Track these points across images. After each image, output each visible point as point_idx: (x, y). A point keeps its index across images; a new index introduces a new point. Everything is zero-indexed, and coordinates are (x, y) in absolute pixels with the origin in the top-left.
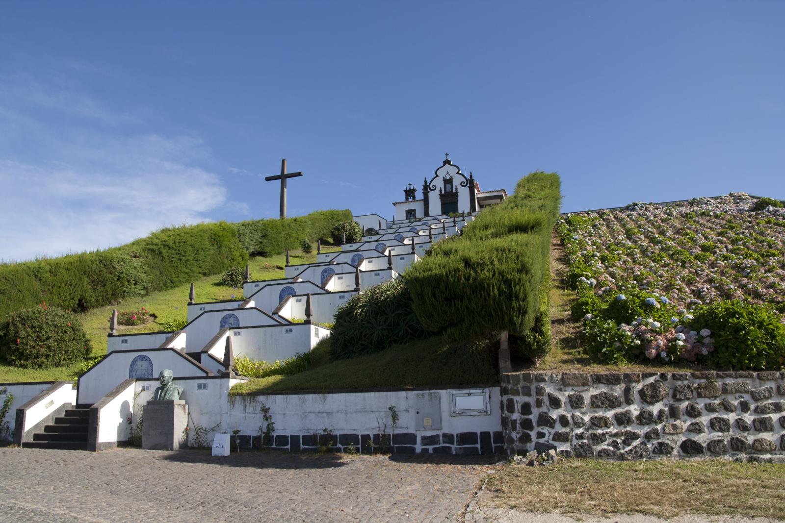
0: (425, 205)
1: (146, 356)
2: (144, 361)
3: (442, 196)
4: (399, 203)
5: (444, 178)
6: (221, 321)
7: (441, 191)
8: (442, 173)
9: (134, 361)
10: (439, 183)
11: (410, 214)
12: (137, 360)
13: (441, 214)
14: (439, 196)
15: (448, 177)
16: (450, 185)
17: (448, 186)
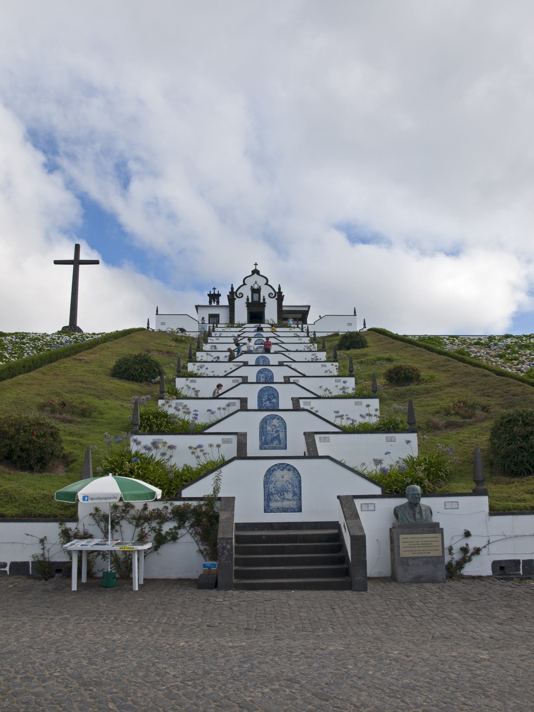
0: (230, 311)
1: (288, 465)
2: (285, 471)
3: (248, 305)
4: (202, 306)
5: (251, 287)
6: (261, 422)
7: (248, 299)
8: (250, 282)
9: (270, 471)
10: (247, 292)
11: (215, 319)
12: (274, 470)
13: (247, 323)
14: (246, 305)
15: (256, 287)
16: (257, 295)
17: (256, 296)
